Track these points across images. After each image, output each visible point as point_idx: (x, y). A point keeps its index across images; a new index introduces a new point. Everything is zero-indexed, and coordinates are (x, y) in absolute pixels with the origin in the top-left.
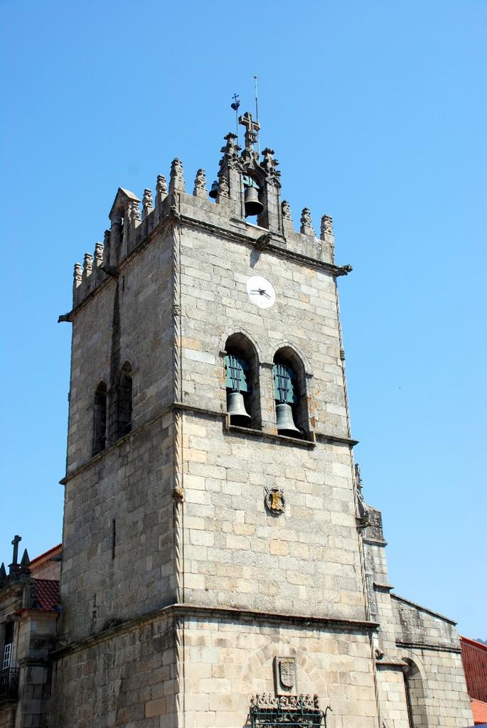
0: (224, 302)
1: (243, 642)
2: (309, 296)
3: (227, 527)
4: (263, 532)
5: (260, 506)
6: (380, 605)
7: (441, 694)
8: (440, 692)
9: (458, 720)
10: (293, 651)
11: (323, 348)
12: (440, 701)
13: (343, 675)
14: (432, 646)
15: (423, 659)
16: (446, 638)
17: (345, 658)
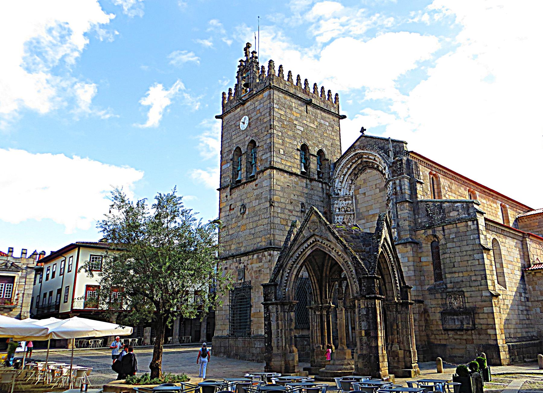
0: (233, 138)
1: (231, 267)
2: (260, 109)
3: (230, 227)
4: (239, 224)
5: (239, 214)
6: (399, 213)
7: (458, 249)
8: (456, 248)
9: (469, 262)
10: (245, 266)
11: (264, 129)
12: (456, 253)
13: (260, 271)
14: (450, 222)
15: (444, 232)
16: (464, 214)
17: (261, 264)
